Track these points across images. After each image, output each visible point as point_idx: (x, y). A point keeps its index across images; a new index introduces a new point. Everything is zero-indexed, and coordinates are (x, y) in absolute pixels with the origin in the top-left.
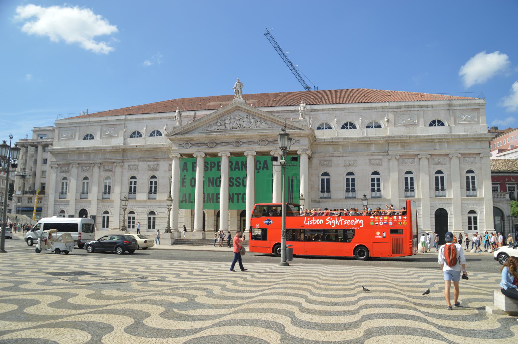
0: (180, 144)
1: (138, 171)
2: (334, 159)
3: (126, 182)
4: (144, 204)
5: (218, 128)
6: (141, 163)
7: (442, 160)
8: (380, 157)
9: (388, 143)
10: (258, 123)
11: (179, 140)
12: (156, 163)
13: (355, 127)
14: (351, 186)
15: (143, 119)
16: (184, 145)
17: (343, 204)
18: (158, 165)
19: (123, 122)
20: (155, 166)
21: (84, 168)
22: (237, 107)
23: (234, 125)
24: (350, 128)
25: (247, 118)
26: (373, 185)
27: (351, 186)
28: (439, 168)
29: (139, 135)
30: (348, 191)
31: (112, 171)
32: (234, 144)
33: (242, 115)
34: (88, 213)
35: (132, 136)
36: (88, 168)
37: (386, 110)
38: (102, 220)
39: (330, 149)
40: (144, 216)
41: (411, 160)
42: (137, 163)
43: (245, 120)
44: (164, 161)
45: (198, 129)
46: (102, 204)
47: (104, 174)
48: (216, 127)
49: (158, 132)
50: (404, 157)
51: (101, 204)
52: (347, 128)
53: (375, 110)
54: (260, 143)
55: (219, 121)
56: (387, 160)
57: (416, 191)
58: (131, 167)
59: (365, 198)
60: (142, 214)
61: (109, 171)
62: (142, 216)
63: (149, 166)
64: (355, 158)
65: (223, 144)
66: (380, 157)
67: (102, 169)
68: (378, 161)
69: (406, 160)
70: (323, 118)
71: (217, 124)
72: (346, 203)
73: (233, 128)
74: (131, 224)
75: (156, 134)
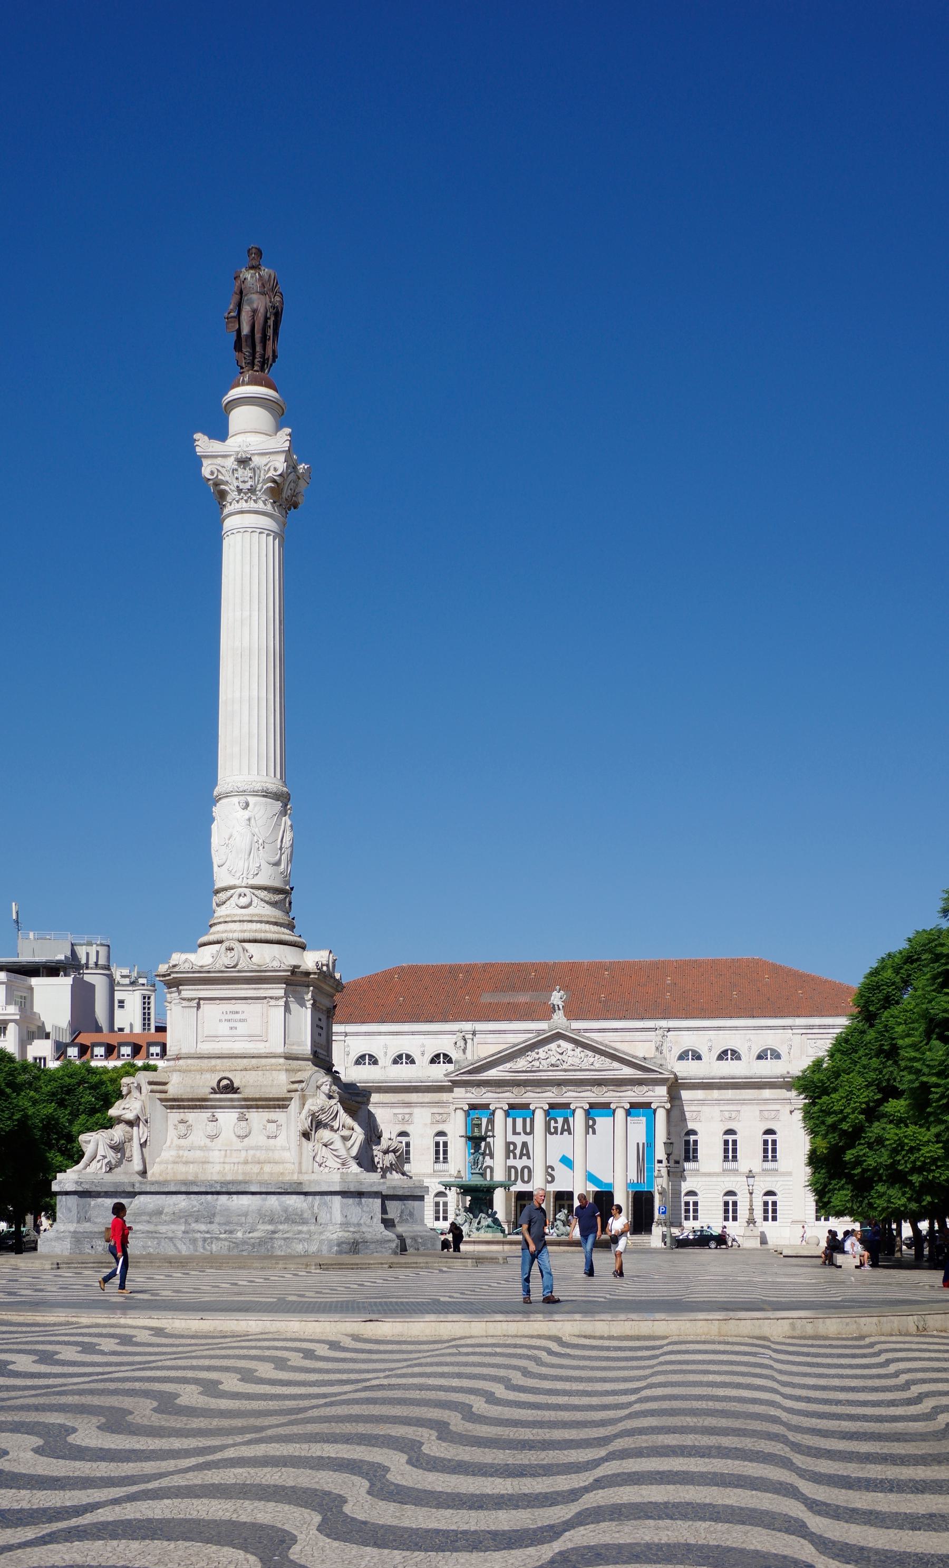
2: (705, 1109)
12: (407, 1110)
13: (739, 1058)
14: (730, 1151)
15: (380, 1033)
17: (719, 1179)
19: (343, 1038)
20: (407, 1116)
23: (553, 1060)
24: (732, 1059)
26: (765, 1151)
27: (730, 1151)
29: (374, 1061)
30: (726, 1158)
35: (360, 1060)
39: (700, 1094)
43: (570, 1053)
49: (408, 1056)
52: (727, 1059)
59: (750, 1175)
64: (738, 1108)
70: (688, 1040)
72: (723, 1179)
73: (552, 1065)
75: (404, 1060)
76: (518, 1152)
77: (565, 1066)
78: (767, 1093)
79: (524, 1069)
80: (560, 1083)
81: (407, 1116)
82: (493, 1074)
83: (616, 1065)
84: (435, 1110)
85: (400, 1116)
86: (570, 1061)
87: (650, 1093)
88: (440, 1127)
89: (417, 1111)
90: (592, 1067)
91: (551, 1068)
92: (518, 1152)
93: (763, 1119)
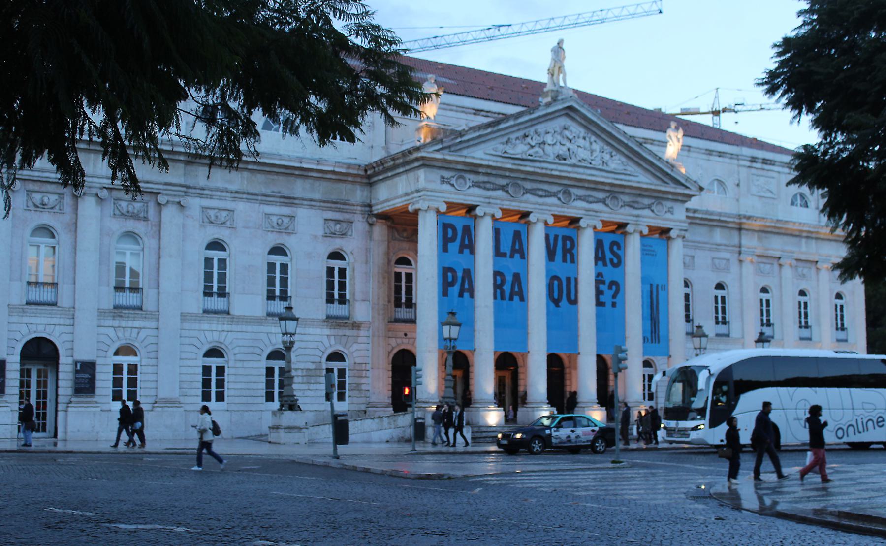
0: (443, 177)
1: (232, 228)
3: (197, 254)
4: (256, 328)
5: (531, 151)
6: (241, 207)
7: (805, 271)
8: (726, 255)
9: (740, 229)
10: (607, 157)
11: (445, 165)
12: (286, 210)
16: (453, 181)
18: (292, 217)
21: (37, 197)
22: (570, 108)
23: (562, 150)
25: (584, 138)
28: (803, 286)
31: (146, 219)
32: (560, 196)
33: (574, 130)
34: (62, 352)
36: (53, 198)
37: (736, 162)
38: (200, 378)
40: (256, 365)
41: (768, 266)
42: (229, 205)
43: (581, 142)
44: (311, 206)
45: (483, 146)
46: (116, 323)
47: (118, 226)
48: (526, 148)
50: (760, 260)
51: (109, 322)
53: (720, 159)
54: (608, 201)
55: (532, 131)
56: (737, 262)
57: (814, 328)
58: (212, 213)
60: (250, 357)
61: (135, 217)
62: (250, 364)
63: (268, 215)
65: (541, 193)
66: (726, 255)
67: (109, 208)
68: (724, 262)
69: (762, 265)
71: (528, 140)
74: (213, 389)
76: (507, 288)
77: (573, 161)
78: (718, 236)
79: (524, 157)
80: (566, 187)
81: (286, 220)
82: (479, 155)
83: (632, 168)
84: (330, 215)
85: (274, 219)
86: (583, 154)
87: (668, 215)
88: (337, 244)
89: (302, 213)
90: (605, 168)
91: (557, 161)
92: (507, 288)
93: (715, 268)
